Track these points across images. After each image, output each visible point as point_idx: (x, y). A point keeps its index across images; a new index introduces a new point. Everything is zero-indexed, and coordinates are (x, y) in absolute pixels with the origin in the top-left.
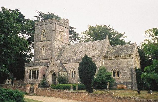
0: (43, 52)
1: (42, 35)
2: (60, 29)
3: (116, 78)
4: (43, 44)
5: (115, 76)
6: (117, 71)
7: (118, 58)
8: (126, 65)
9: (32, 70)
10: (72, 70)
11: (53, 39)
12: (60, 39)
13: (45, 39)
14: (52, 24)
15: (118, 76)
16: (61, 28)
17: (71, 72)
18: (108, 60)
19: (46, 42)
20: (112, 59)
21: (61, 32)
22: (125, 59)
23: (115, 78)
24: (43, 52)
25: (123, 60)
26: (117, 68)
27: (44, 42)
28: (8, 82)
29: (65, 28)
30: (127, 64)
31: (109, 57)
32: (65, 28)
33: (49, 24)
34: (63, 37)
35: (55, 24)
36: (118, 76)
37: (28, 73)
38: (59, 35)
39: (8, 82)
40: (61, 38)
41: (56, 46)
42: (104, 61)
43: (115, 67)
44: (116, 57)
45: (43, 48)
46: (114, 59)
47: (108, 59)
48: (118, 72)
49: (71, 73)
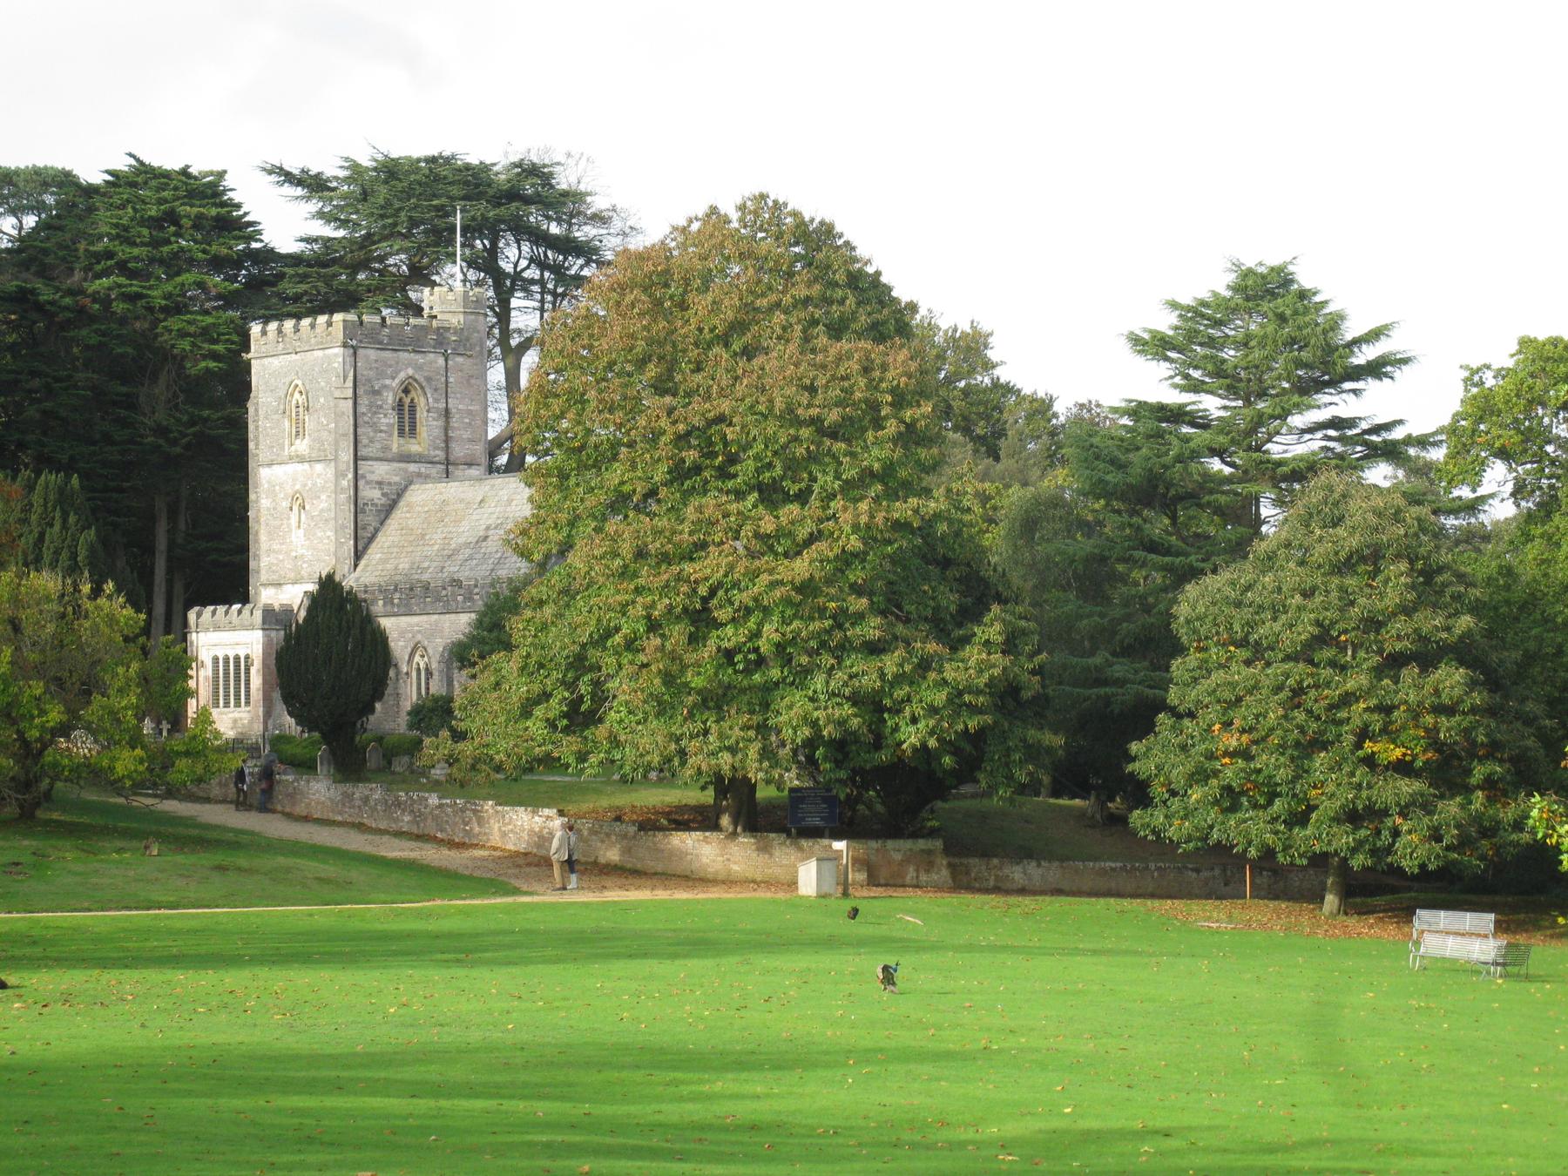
0: (297, 538)
2: (402, 375)
4: (295, 480)
10: (417, 658)
12: (396, 444)
16: (409, 365)
19: (306, 466)
21: (413, 394)
27: (299, 467)
32: (441, 361)
33: (320, 353)
34: (428, 426)
38: (389, 419)
40: (408, 427)
45: (295, 508)
49: (414, 674)
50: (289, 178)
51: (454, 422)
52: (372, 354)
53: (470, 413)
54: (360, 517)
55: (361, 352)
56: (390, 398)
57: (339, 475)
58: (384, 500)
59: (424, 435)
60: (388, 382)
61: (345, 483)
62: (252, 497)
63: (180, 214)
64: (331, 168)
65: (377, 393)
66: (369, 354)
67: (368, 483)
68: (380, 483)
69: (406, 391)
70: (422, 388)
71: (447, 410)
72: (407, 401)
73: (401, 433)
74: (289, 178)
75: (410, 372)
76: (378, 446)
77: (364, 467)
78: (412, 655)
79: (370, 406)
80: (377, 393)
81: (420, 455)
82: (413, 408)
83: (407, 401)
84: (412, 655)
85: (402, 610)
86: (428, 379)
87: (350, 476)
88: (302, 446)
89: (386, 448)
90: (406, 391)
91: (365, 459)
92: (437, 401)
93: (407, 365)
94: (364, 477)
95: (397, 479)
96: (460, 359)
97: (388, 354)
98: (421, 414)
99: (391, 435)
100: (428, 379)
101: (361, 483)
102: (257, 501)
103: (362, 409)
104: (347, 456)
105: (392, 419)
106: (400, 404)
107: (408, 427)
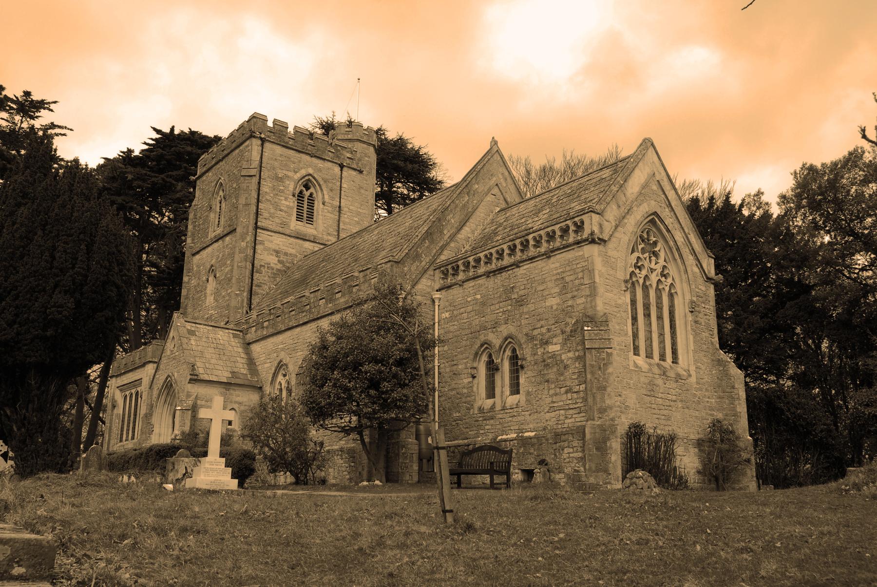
1: (212, 215)
2: (303, 172)
3: (498, 407)
5: (498, 391)
6: (508, 353)
7: (512, 260)
8: (553, 302)
9: (127, 393)
10: (280, 378)
11: (245, 221)
12: (295, 225)
13: (219, 231)
14: (248, 146)
15: (515, 389)
17: (277, 386)
18: (461, 284)
19: (220, 242)
20: (482, 270)
21: (312, 190)
22: (548, 255)
23: (493, 406)
24: (210, 300)
25: (540, 264)
26: (505, 330)
27: (216, 245)
29: (342, 166)
30: (560, 294)
31: (467, 265)
32: (337, 169)
34: (324, 215)
35: (263, 141)
36: (515, 389)
37: (115, 411)
41: (265, 257)
42: (437, 295)
43: (495, 325)
44: (500, 255)
46: (488, 274)
47: (461, 276)
48: (514, 359)
51: (344, 218)
52: (279, 150)
53: (359, 214)
54: (256, 276)
55: (267, 145)
58: (279, 266)
59: (320, 222)
60: (290, 174)
62: (185, 279)
67: (267, 249)
69: (307, 187)
70: (319, 185)
71: (340, 207)
73: (299, 218)
75: (311, 171)
76: (277, 221)
77: (262, 235)
78: (275, 375)
79: (274, 188)
80: (280, 180)
81: (315, 237)
84: (275, 375)
85: (271, 331)
87: (249, 238)
89: (284, 224)
92: (332, 199)
94: (262, 243)
95: (293, 251)
96: (354, 173)
98: (318, 206)
99: (290, 215)
102: (188, 283)
105: (292, 203)
106: (301, 195)
107: (306, 213)
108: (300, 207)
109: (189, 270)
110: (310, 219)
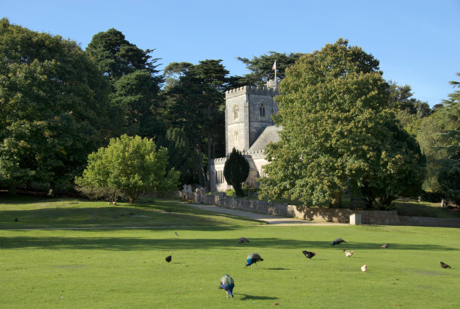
2: (261, 101)
12: (260, 118)
21: (264, 106)
27: (236, 124)
28: (187, 188)
32: (271, 97)
38: (258, 112)
39: (187, 188)
50: (239, 59)
55: (250, 95)
56: (258, 107)
57: (246, 126)
58: (256, 132)
61: (247, 127)
62: (226, 133)
63: (214, 70)
64: (251, 59)
65: (255, 105)
66: (253, 96)
68: (256, 128)
69: (262, 105)
72: (262, 107)
73: (261, 115)
74: (239, 59)
75: (263, 100)
80: (255, 105)
82: (264, 109)
83: (262, 107)
86: (268, 102)
88: (237, 120)
90: (262, 105)
91: (251, 121)
92: (270, 107)
93: (262, 99)
97: (257, 96)
98: (266, 111)
99: (258, 116)
100: (268, 102)
101: (251, 128)
103: (251, 109)
104: (247, 120)
106: (261, 108)
108: (261, 112)
109: (227, 130)
110: (264, 115)
